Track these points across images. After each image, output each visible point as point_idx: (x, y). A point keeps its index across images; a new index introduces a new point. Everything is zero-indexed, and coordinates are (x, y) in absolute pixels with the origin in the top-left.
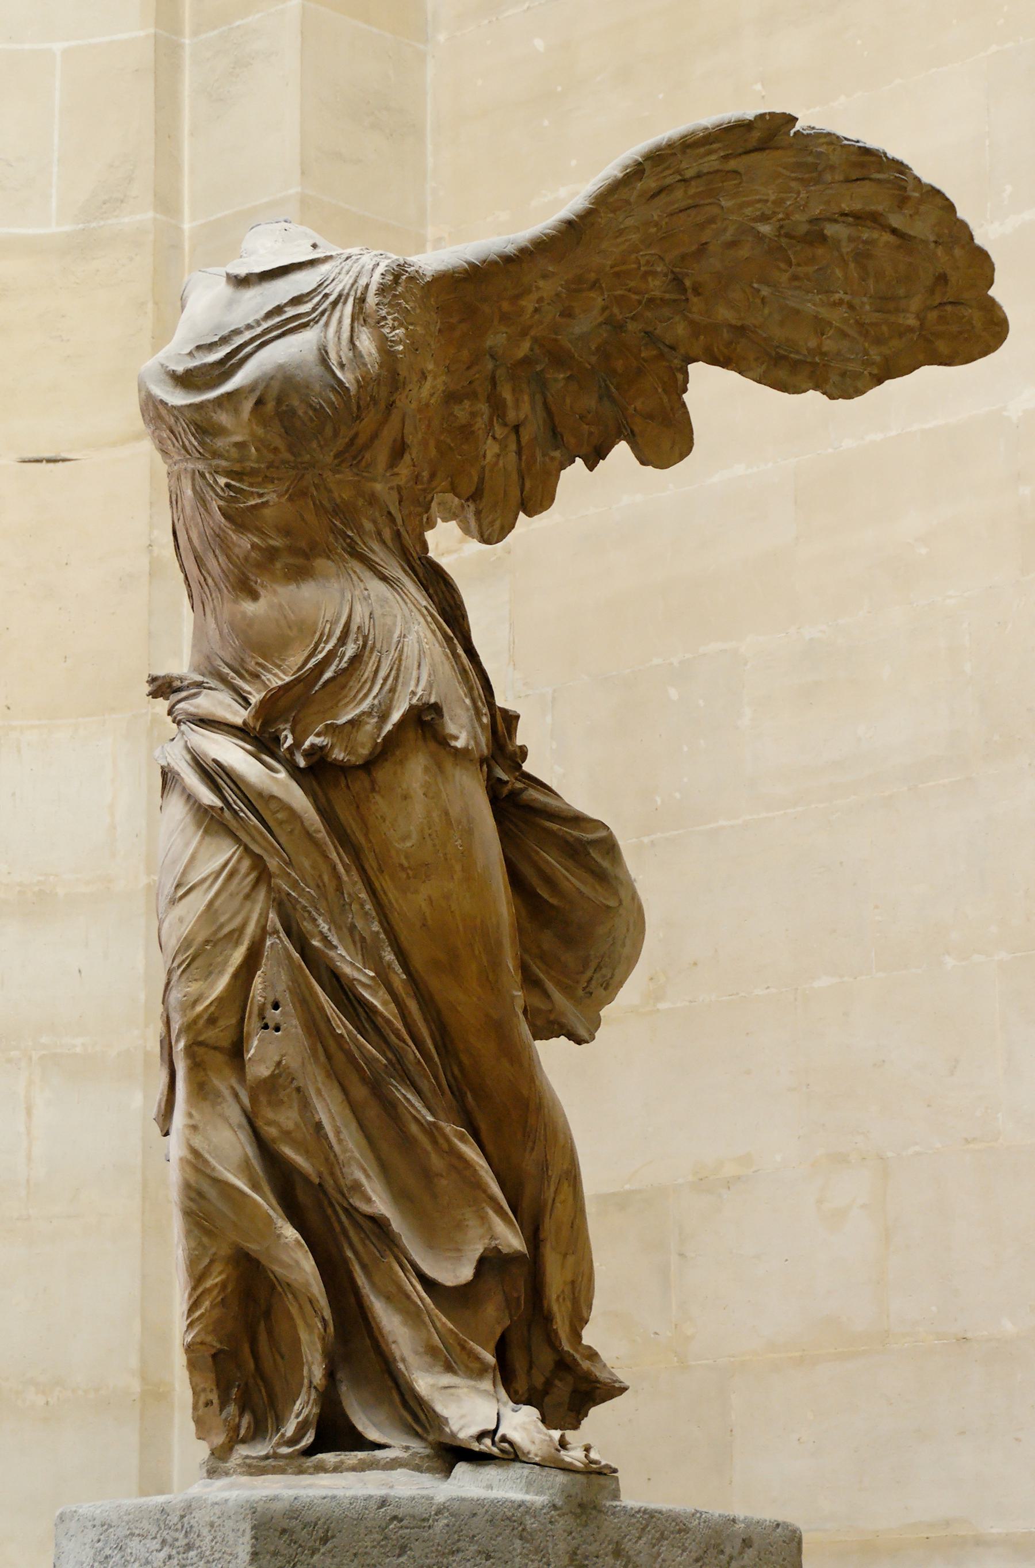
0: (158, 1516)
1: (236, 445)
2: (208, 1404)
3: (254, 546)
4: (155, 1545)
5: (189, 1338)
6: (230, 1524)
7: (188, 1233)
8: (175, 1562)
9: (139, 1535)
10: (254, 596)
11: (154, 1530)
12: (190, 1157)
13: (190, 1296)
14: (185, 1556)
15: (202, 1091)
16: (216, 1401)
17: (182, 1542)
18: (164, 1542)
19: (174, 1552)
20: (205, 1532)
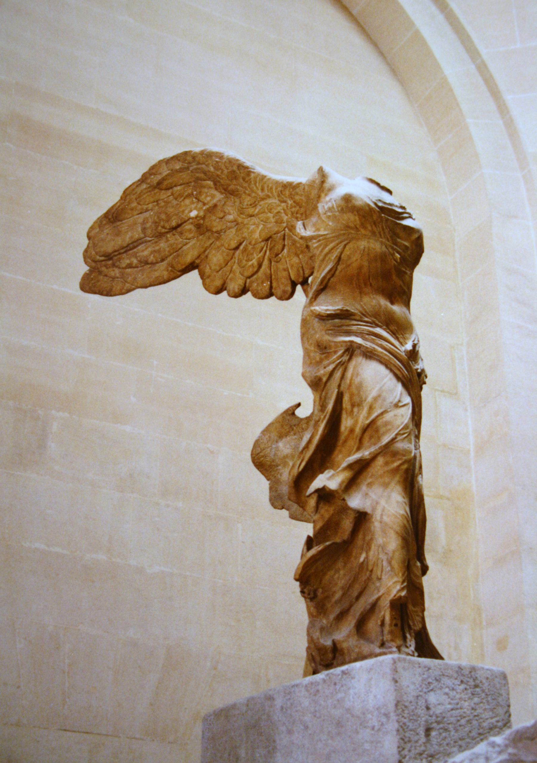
0: (457, 669)
1: (406, 246)
2: (396, 625)
3: (401, 286)
4: (457, 682)
5: (403, 593)
6: (498, 680)
7: (403, 548)
8: (469, 691)
9: (447, 676)
10: (392, 303)
11: (455, 675)
12: (406, 515)
13: (403, 575)
14: (474, 690)
15: (405, 489)
16: (399, 625)
17: (472, 683)
18: (462, 682)
19: (468, 687)
20: (484, 681)
